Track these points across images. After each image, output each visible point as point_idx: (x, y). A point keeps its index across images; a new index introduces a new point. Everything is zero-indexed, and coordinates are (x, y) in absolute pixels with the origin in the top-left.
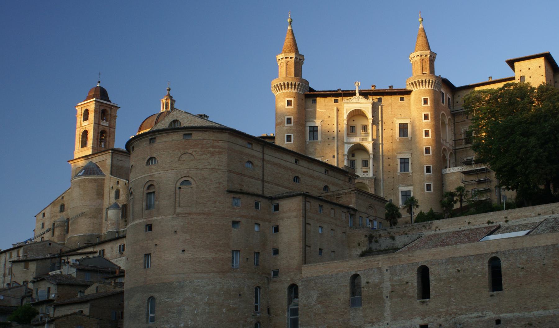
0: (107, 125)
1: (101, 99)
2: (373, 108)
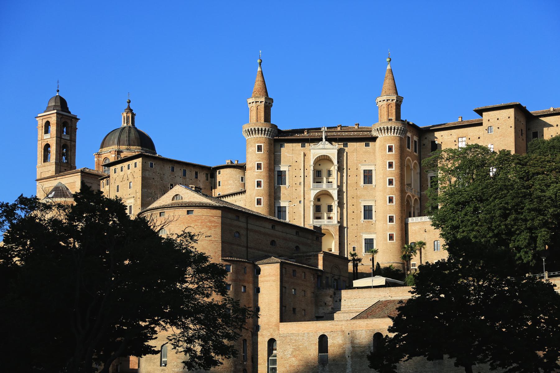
0: (68, 138)
1: (62, 111)
2: (338, 153)
